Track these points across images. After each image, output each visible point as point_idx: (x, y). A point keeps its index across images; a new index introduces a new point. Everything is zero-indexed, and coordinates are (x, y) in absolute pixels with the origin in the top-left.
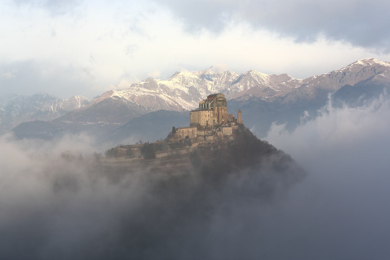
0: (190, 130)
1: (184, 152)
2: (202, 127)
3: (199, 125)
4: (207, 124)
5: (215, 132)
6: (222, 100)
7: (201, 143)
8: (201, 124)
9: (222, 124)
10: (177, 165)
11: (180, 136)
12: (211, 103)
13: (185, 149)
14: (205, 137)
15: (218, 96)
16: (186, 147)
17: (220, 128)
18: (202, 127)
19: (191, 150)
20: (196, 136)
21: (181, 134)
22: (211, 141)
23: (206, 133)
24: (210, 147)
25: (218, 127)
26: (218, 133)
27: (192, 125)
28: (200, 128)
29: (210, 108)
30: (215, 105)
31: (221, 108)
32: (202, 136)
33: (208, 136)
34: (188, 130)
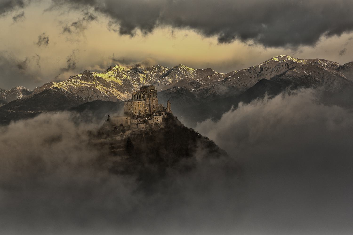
1: (118, 138)
2: (135, 116)
3: (133, 114)
4: (140, 113)
5: (146, 121)
7: (134, 130)
8: (134, 113)
9: (153, 113)
10: (112, 151)
12: (143, 94)
15: (149, 88)
16: (120, 134)
17: (151, 117)
18: (135, 116)
20: (129, 124)
22: (143, 128)
23: (139, 122)
24: (142, 134)
25: (150, 115)
26: (150, 122)
28: (133, 117)
29: (142, 99)
30: (147, 96)
31: (153, 99)
32: (135, 124)
33: (140, 124)
34: (122, 119)
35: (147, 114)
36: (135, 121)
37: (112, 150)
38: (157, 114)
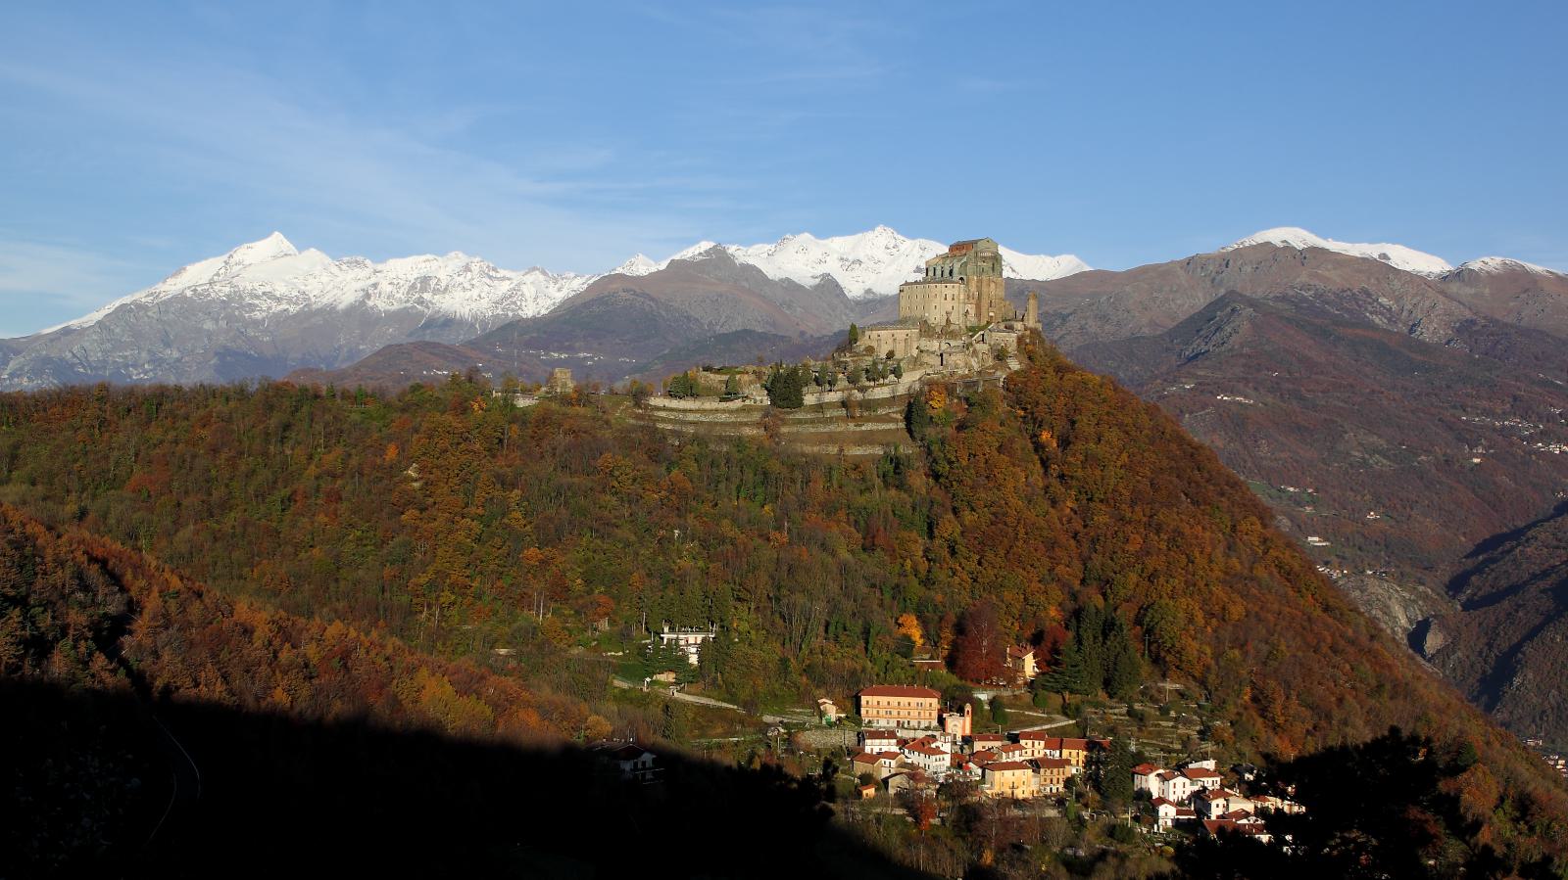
0: (901, 334)
1: (881, 393)
2: (934, 328)
4: (948, 321)
6: (991, 258)
8: (931, 321)
9: (988, 323)
10: (863, 428)
11: (870, 350)
13: (883, 385)
14: (941, 355)
16: (886, 381)
18: (934, 328)
19: (901, 390)
20: (915, 352)
21: (874, 344)
23: (944, 347)
27: (903, 323)
29: (956, 277)
32: (933, 353)
35: (969, 325)
36: (935, 345)
37: (861, 425)
38: (1002, 327)
